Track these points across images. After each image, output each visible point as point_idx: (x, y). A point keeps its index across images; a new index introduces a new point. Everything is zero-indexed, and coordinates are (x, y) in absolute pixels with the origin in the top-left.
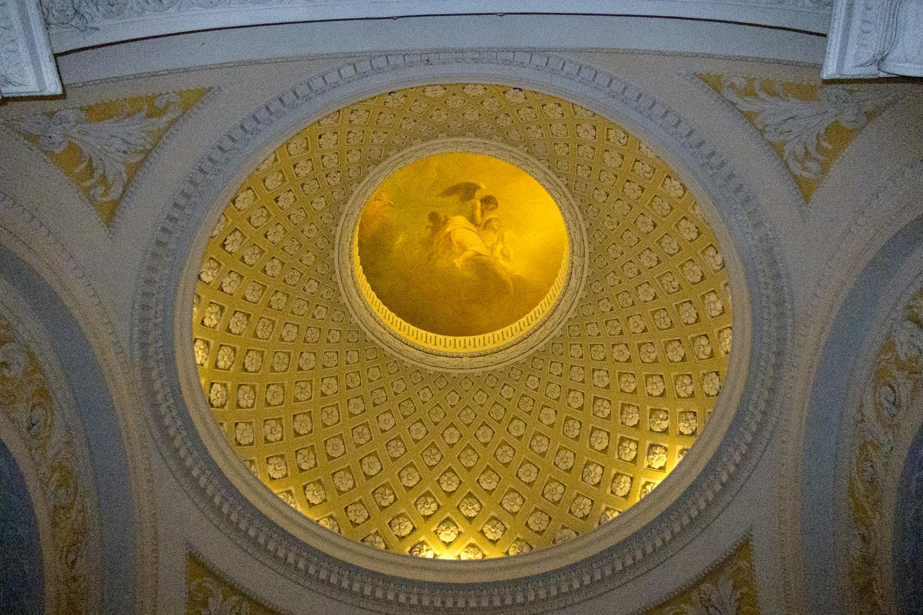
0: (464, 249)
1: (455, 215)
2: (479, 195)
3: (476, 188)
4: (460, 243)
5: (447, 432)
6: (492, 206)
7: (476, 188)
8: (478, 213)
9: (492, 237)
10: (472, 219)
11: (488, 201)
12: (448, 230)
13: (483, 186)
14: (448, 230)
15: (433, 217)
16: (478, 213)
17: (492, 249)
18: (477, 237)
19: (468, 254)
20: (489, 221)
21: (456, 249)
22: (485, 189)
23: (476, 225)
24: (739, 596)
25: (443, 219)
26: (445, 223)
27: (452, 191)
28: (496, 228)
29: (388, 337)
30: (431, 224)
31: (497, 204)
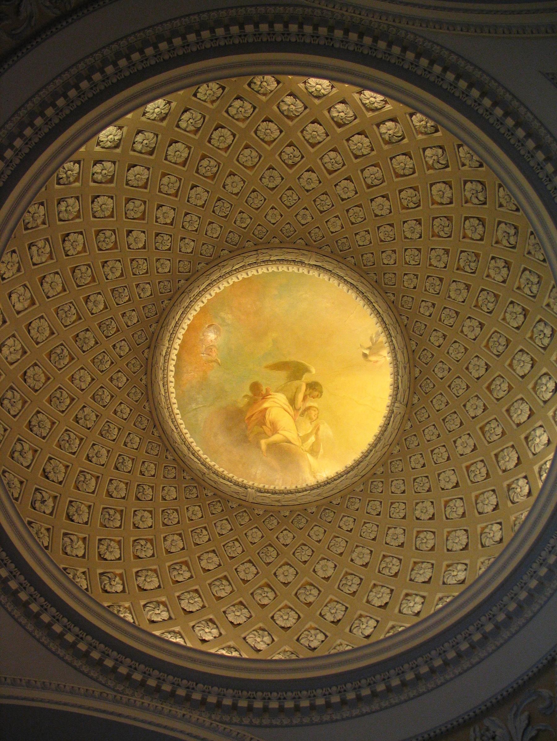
0: (275, 430)
2: (307, 378)
3: (306, 370)
4: (273, 424)
5: (205, 556)
6: (316, 393)
8: (300, 396)
9: (307, 427)
10: (292, 401)
12: (265, 405)
13: (313, 370)
14: (265, 405)
15: (255, 387)
16: (300, 396)
17: (304, 439)
18: (292, 421)
19: (276, 438)
20: (309, 408)
21: (267, 429)
22: (314, 373)
23: (296, 409)
24: (534, 733)
25: (264, 392)
26: (264, 397)
28: (314, 418)
30: (250, 394)
31: (321, 392)
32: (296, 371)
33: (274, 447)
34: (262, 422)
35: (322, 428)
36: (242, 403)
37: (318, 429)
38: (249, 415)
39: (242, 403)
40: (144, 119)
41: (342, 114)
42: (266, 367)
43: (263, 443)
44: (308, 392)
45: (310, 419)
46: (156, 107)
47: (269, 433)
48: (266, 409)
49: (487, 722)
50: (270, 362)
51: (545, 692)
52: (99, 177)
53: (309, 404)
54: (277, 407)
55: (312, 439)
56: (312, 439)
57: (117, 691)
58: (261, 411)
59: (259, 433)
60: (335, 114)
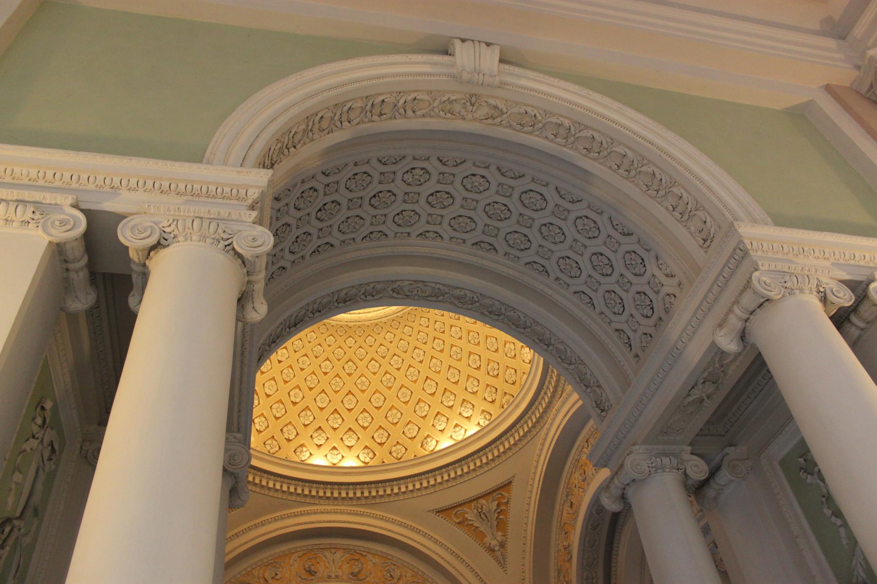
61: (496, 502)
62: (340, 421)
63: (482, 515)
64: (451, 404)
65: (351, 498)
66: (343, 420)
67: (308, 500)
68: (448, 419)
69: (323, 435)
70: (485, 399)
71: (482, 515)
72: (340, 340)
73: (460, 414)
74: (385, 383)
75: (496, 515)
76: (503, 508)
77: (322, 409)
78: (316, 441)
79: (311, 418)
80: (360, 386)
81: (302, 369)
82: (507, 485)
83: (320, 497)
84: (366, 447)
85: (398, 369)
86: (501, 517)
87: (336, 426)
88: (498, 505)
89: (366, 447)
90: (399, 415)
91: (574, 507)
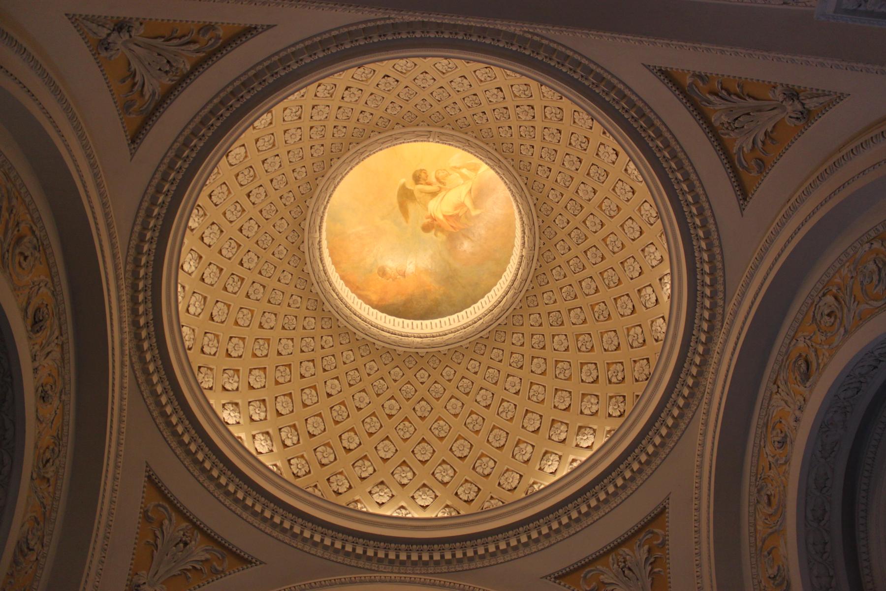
0: (462, 205)
1: (427, 209)
2: (410, 185)
3: (403, 188)
4: (456, 208)
6: (423, 175)
7: (403, 188)
10: (434, 194)
11: (417, 178)
12: (441, 217)
13: (403, 180)
14: (441, 217)
15: (426, 228)
17: (465, 178)
19: (468, 203)
20: (437, 179)
21: (461, 212)
23: (440, 191)
25: (429, 220)
26: (434, 219)
27: (404, 211)
29: (487, 318)
30: (433, 232)
31: (421, 170)
32: (405, 196)
33: (476, 203)
34: (456, 217)
35: (453, 164)
36: (442, 237)
37: (455, 167)
38: (451, 230)
39: (442, 237)
40: (242, 422)
41: (192, 263)
42: (407, 222)
43: (474, 213)
44: (423, 182)
45: (447, 176)
46: (229, 416)
47: (465, 209)
48: (444, 216)
49: (717, 124)
50: (402, 219)
51: (689, 81)
52: (295, 439)
53: (432, 178)
54: (440, 207)
55: (464, 171)
56: (464, 171)
57: (702, 397)
58: (447, 220)
59: (466, 218)
60: (193, 268)
61: (646, 547)
62: (410, 475)
63: (625, 569)
64: (563, 436)
65: (426, 564)
66: (414, 474)
67: (361, 563)
68: (560, 457)
69: (387, 490)
70: (610, 415)
71: (627, 572)
72: (410, 374)
73: (577, 446)
74: (471, 426)
75: (649, 568)
76: (658, 554)
77: (385, 460)
78: (376, 498)
79: (371, 470)
80: (436, 432)
81: (359, 409)
82: (659, 515)
83: (380, 561)
84: (447, 506)
85: (488, 407)
86: (656, 570)
87: (405, 481)
88: (649, 551)
89: (447, 506)
90: (491, 464)
91: (775, 501)
